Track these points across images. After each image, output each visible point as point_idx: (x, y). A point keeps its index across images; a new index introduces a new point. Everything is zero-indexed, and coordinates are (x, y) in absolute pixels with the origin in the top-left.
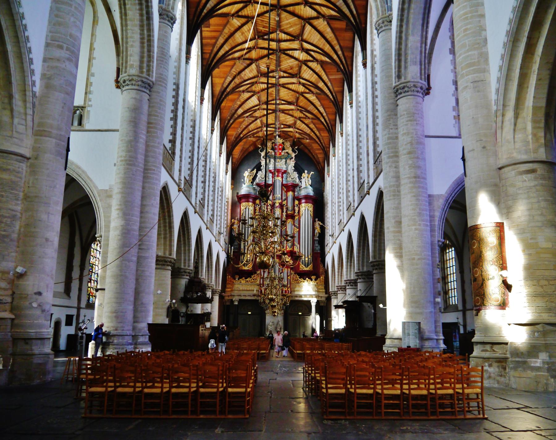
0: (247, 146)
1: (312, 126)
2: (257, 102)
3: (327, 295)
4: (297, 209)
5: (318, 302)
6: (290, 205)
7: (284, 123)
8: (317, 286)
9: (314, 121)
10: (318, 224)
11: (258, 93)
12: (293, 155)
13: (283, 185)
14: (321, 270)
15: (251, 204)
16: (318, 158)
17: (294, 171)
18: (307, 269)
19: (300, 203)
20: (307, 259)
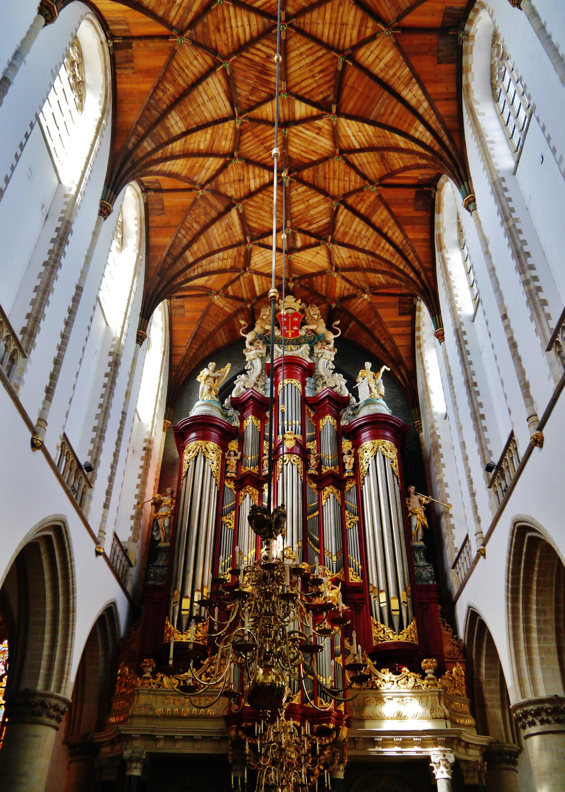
0: (209, 327)
1: (381, 216)
2: (224, 108)
3: (483, 740)
4: (349, 460)
5: (457, 769)
6: (328, 452)
7: (303, 226)
8: (445, 697)
9: (389, 194)
10: (416, 503)
11: (226, 58)
12: (331, 337)
13: (304, 400)
14: (447, 648)
15: (211, 445)
16: (395, 348)
17: (335, 371)
18: (402, 638)
19: (357, 445)
20: (395, 604)
